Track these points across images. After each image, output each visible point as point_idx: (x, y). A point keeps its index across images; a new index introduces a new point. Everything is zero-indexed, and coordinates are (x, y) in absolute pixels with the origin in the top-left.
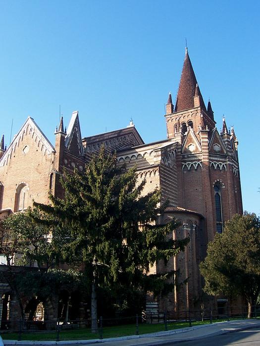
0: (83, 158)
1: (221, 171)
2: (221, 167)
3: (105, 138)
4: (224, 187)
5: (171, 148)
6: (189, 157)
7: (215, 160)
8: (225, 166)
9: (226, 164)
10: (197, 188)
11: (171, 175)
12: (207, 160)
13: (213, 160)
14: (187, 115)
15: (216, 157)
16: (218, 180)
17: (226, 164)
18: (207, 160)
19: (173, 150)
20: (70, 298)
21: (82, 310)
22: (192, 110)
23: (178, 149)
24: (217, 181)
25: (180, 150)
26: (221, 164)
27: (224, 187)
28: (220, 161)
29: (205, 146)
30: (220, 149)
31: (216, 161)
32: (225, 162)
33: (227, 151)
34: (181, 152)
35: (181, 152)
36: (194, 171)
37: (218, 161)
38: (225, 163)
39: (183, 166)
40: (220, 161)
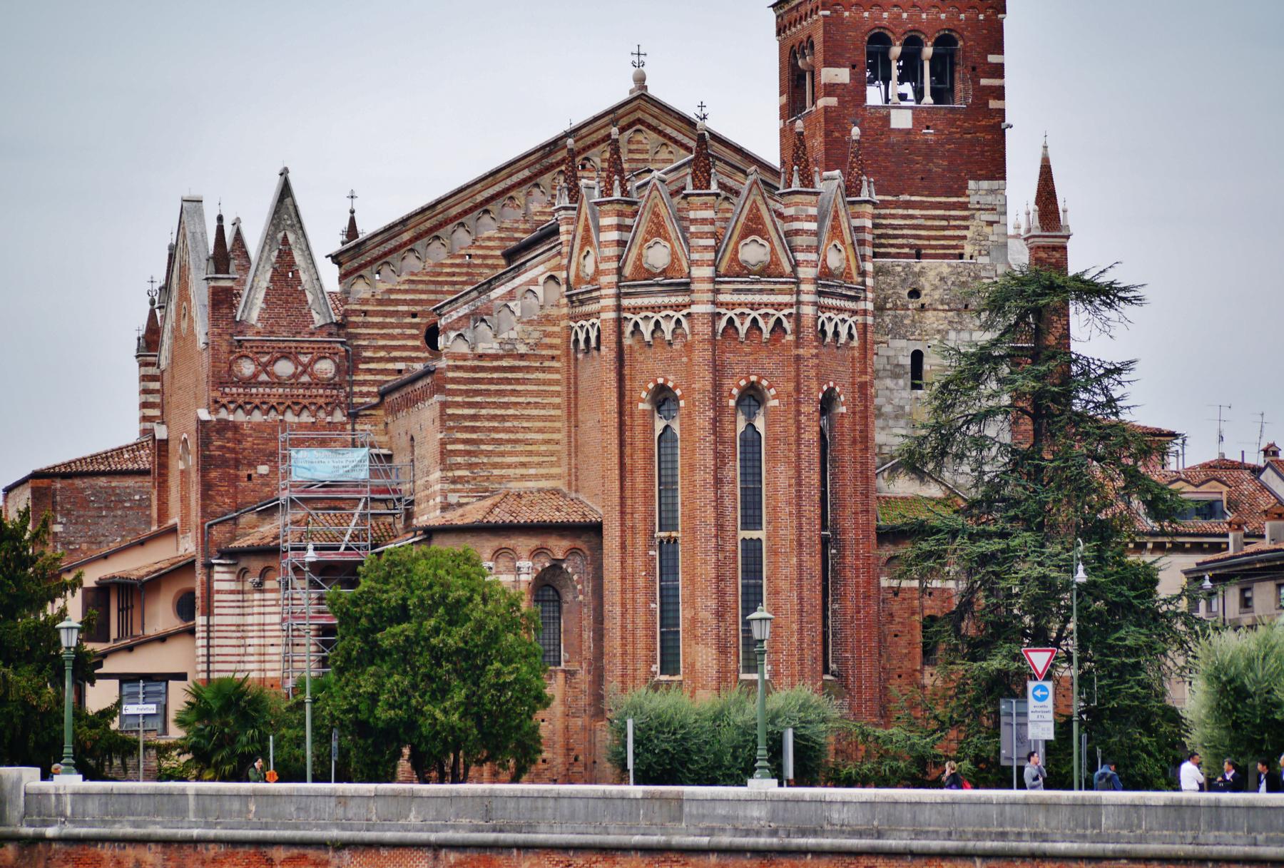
0: (334, 330)
1: (670, 344)
2: (668, 327)
3: (454, 211)
5: (517, 281)
6: (582, 303)
11: (517, 381)
12: (612, 315)
13: (636, 310)
16: (660, 381)
17: (689, 314)
19: (534, 282)
23: (559, 267)
24: (657, 385)
25: (564, 274)
28: (665, 307)
29: (609, 259)
30: (670, 258)
32: (685, 306)
34: (567, 281)
35: (567, 281)
36: (595, 353)
38: (685, 312)
39: (573, 338)
40: (665, 307)
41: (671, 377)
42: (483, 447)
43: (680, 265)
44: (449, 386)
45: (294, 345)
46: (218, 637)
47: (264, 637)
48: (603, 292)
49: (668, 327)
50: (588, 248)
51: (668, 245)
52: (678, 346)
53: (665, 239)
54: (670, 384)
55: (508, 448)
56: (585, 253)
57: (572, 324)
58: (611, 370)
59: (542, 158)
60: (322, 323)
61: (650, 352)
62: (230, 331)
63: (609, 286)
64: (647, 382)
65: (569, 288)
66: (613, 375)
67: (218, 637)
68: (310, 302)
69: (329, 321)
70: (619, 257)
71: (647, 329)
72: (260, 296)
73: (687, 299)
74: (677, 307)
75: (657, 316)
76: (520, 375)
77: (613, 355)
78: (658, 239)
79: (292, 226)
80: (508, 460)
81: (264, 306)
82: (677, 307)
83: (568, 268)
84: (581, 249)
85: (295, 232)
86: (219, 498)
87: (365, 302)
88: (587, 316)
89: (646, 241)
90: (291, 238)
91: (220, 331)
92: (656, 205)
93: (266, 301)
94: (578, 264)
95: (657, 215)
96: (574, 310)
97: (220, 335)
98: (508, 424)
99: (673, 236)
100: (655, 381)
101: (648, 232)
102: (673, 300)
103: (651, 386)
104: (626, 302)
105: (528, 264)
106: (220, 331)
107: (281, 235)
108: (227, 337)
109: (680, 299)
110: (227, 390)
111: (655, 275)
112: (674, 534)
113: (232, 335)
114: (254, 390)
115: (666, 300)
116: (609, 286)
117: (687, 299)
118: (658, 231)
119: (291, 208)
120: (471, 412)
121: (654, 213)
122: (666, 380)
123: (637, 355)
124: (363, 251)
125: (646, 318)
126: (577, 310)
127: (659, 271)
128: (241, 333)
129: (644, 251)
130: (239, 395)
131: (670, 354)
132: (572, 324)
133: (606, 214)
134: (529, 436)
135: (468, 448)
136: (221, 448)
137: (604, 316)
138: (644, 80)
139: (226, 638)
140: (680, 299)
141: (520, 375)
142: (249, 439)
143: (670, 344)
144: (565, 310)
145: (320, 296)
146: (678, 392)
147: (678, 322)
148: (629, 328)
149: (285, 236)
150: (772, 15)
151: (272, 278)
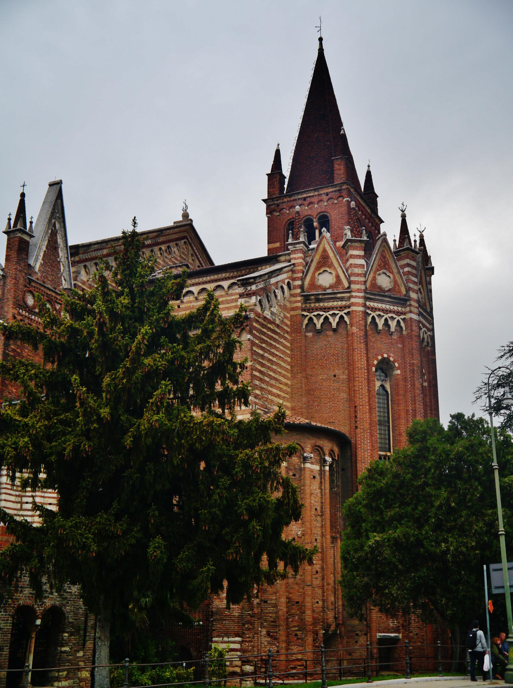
1: (391, 334)
2: (393, 324)
4: (399, 372)
6: (318, 300)
7: (379, 310)
8: (402, 324)
9: (404, 319)
10: (337, 372)
11: (275, 340)
12: (361, 309)
13: (374, 309)
14: (315, 200)
15: (382, 301)
16: (385, 356)
18: (361, 309)
19: (283, 281)
20: (38, 622)
21: (65, 652)
22: (325, 191)
25: (298, 283)
26: (392, 318)
27: (399, 372)
28: (390, 311)
30: (393, 284)
31: (383, 310)
33: (408, 289)
34: (302, 287)
36: (331, 333)
37: (386, 311)
38: (403, 317)
39: (306, 321)
40: (390, 311)
41: (392, 355)
42: (266, 378)
43: (399, 289)
44: (254, 332)
45: (54, 294)
46: (6, 493)
47: (44, 497)
48: (354, 294)
49: (393, 324)
50: (327, 269)
51: (391, 276)
52: (395, 337)
53: (390, 272)
54: (392, 359)
55: (273, 382)
56: (321, 271)
57: (305, 313)
58: (360, 343)
59: (157, 237)
60: (66, 287)
61: (378, 337)
62: (25, 271)
63: (358, 291)
64: (377, 355)
65: (303, 291)
66: (363, 346)
67: (6, 493)
68: (62, 271)
69: (69, 287)
70: (365, 275)
71: (380, 323)
72: (42, 254)
73: (404, 310)
74: (398, 313)
75: (386, 316)
76: (277, 337)
77: (362, 334)
78: (385, 271)
79: (59, 218)
80: (274, 391)
81: (42, 262)
82: (398, 313)
83: (303, 279)
84: (317, 268)
85: (60, 223)
86: (10, 387)
87: (84, 283)
88: (326, 309)
89: (378, 270)
90: (57, 226)
91: (20, 268)
92: (384, 251)
93: (43, 259)
94: (313, 278)
95: (385, 257)
96: (308, 305)
97: (20, 271)
98: (274, 367)
99: (395, 271)
100: (382, 356)
101: (379, 265)
102: (396, 308)
103: (380, 358)
104: (368, 303)
105: (284, 270)
106: (20, 268)
107: (53, 221)
108: (24, 275)
109: (400, 309)
110: (21, 311)
111: (384, 291)
112: (389, 454)
113: (26, 275)
114: (33, 317)
115: (392, 307)
116: (358, 291)
117: (404, 310)
118: (384, 265)
119: (60, 207)
120: (261, 352)
121: (382, 255)
122: (389, 356)
123: (371, 337)
124: (89, 250)
125: (379, 316)
126: (312, 305)
127: (386, 289)
128: (30, 275)
129: (377, 276)
130: (26, 316)
131: (390, 341)
132: (305, 313)
133: (356, 248)
134: (281, 378)
135: (261, 376)
136: (14, 351)
137: (353, 308)
138: (188, 216)
139: (10, 494)
140: (400, 309)
141: (277, 337)
142: (26, 351)
143: (391, 334)
144: (299, 304)
145: (67, 269)
146: (396, 364)
147: (398, 322)
148: (369, 319)
149: (55, 223)
150: (264, 205)
151: (47, 245)
